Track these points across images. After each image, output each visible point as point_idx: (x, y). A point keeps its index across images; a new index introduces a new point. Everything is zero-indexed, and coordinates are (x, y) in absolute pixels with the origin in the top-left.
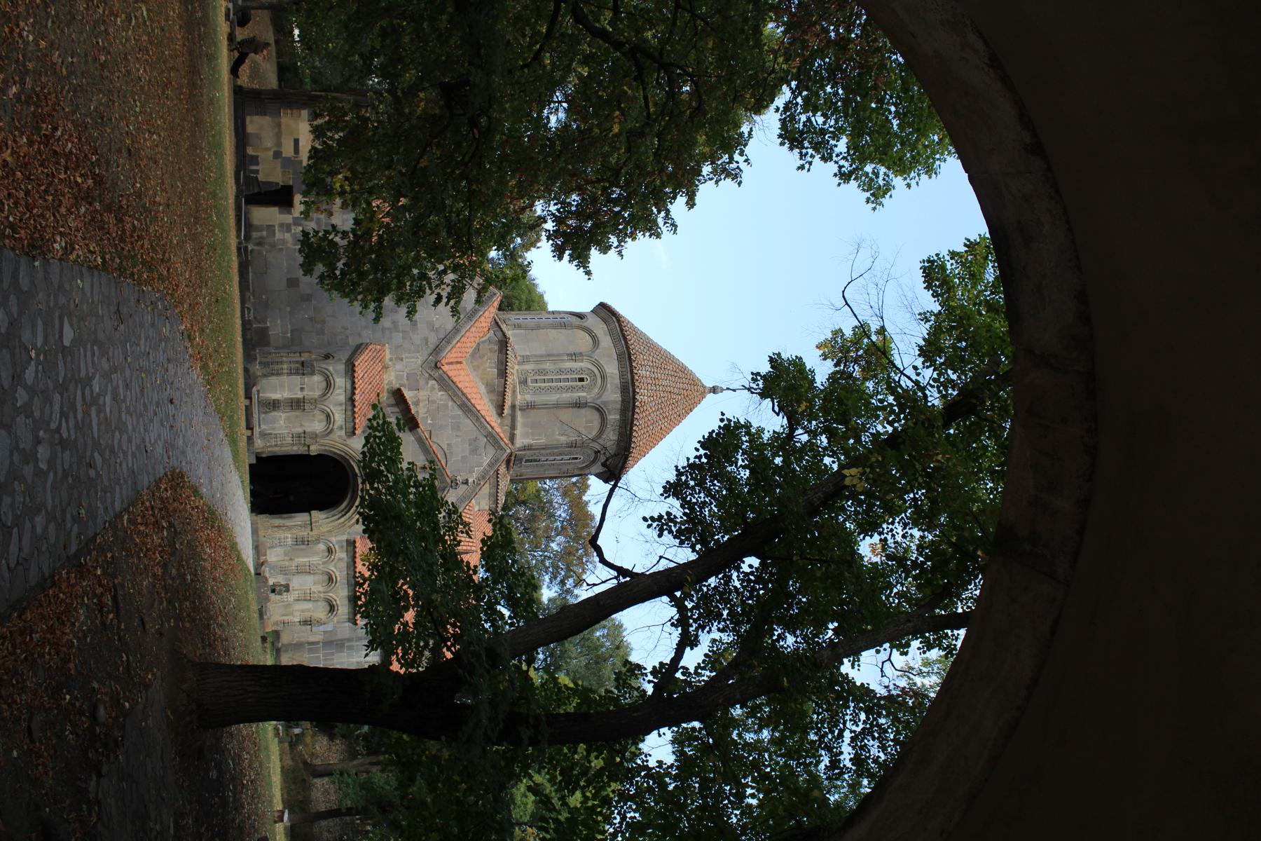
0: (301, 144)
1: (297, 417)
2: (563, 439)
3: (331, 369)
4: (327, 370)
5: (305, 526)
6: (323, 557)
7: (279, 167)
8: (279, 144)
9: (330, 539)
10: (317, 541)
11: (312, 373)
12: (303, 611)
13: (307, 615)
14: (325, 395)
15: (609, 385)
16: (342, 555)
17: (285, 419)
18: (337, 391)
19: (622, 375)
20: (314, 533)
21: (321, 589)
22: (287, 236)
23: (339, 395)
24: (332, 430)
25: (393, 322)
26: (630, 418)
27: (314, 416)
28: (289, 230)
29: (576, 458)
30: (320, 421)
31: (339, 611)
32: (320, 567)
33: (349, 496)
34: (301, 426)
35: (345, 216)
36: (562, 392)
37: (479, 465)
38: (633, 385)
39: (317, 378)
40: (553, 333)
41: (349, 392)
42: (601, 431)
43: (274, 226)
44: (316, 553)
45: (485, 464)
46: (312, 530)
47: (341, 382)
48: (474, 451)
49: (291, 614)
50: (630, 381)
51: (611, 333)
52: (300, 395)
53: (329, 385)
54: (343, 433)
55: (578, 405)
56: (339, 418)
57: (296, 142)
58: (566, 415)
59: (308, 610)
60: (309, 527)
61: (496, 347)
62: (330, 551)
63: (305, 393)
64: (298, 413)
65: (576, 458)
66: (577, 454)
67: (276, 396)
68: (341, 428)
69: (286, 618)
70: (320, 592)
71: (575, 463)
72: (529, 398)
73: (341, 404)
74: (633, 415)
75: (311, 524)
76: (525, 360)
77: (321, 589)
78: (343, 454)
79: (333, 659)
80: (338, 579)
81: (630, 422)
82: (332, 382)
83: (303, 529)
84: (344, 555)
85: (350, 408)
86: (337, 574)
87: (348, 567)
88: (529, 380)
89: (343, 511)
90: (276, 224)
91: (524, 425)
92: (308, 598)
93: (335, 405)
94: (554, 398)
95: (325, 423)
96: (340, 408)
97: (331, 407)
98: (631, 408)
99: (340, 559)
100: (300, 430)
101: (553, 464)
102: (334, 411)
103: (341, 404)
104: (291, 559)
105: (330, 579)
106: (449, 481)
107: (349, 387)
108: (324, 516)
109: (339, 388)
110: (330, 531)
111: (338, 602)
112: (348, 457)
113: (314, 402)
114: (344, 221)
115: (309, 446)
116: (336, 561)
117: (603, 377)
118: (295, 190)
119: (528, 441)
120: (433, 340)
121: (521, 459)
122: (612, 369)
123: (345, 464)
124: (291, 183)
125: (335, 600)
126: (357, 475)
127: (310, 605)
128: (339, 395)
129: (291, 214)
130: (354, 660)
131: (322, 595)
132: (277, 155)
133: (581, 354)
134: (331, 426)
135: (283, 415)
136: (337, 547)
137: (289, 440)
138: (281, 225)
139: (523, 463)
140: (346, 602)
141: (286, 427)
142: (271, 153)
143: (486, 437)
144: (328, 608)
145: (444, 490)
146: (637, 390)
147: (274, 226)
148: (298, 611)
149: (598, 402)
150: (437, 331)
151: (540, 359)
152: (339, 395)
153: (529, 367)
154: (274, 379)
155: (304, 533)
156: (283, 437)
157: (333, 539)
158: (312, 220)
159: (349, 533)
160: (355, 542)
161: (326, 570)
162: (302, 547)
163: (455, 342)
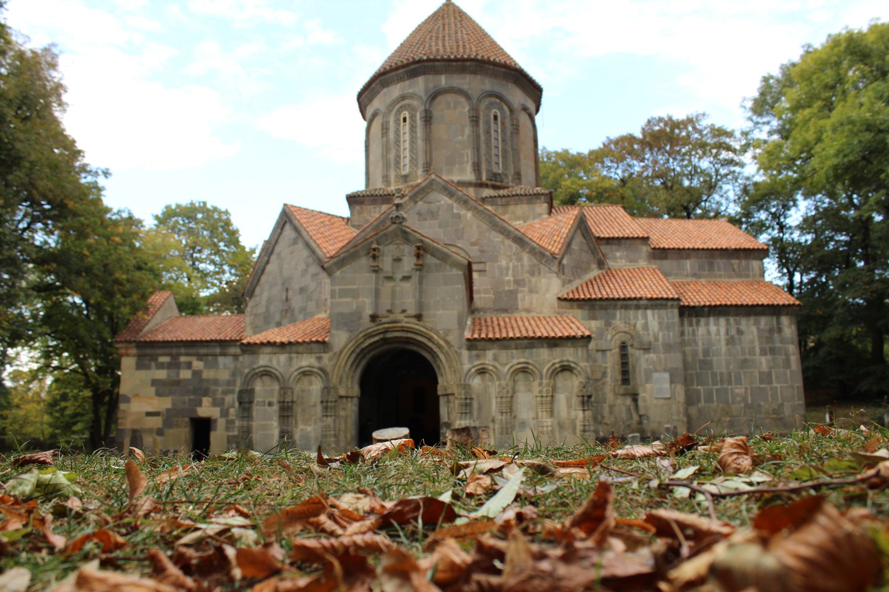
0: (150, 410)
1: (303, 411)
2: (468, 131)
3: (247, 371)
4: (247, 375)
5: (448, 402)
6: (492, 380)
7: (171, 431)
8: (150, 431)
9: (465, 372)
10: (466, 387)
11: (251, 392)
12: (569, 406)
13: (576, 401)
14: (277, 378)
15: (411, 91)
16: (489, 357)
17: (306, 424)
18: (274, 363)
19: (400, 79)
20: (455, 390)
21: (536, 383)
22: (237, 423)
23: (278, 363)
24: (321, 369)
25: (300, 312)
26: (442, 63)
27: (303, 391)
28: (232, 422)
29: (496, 117)
30: (311, 383)
31: (571, 359)
32: (503, 383)
33: (415, 348)
34: (315, 406)
35: (221, 366)
36: (416, 138)
37: (450, 207)
38: (407, 65)
39: (259, 387)
40: (372, 158)
41: (275, 350)
42: (460, 92)
43: (228, 437)
44: (486, 389)
45: (450, 201)
46: (453, 394)
47: (264, 360)
48: (433, 215)
49: (573, 422)
50: (406, 69)
51: (371, 100)
52: (276, 407)
53: (267, 373)
54: (326, 357)
55: (428, 119)
56: (307, 361)
57: (149, 414)
58: (440, 130)
59: (568, 400)
60: (451, 397)
61: (357, 208)
62: (482, 372)
63: (275, 400)
64: (298, 410)
65: (496, 117)
66: (488, 116)
67: (276, 433)
68: (319, 359)
69: (579, 428)
70: (540, 384)
71: (503, 118)
72: (420, 171)
73: (291, 359)
74: (438, 60)
75: (448, 395)
76: (386, 179)
77: (536, 383)
78: (354, 355)
79: (721, 373)
80: (522, 360)
81: (446, 63)
82: (262, 369)
83: (451, 405)
84: (490, 354)
85: (294, 348)
86: (515, 361)
87: (506, 348)
88: (403, 173)
89: (433, 356)
90: (226, 434)
91: (450, 172)
92: (549, 402)
93: (290, 365)
94: (420, 143)
95: (313, 378)
96: (295, 360)
97: (292, 370)
98: (431, 64)
99: (495, 358)
100: (319, 408)
101: (504, 141)
102: (296, 367)
103: (291, 359)
104: (493, 421)
105: (524, 370)
106: (394, 226)
107: (268, 350)
108: (440, 380)
109: (271, 360)
110: (455, 371)
111: (557, 360)
112: (358, 350)
113: (285, 389)
114: (225, 367)
115: (341, 397)
116: (497, 364)
117: (403, 98)
118: (193, 416)
119: (469, 168)
120: (315, 269)
121: (495, 175)
122: (395, 91)
123: (373, 353)
124: (187, 420)
125: (554, 364)
126: (382, 339)
127: (561, 399)
128: (278, 363)
129: (216, 420)
130: (724, 348)
131: (545, 381)
132: (160, 432)
133: (382, 125)
134: (315, 370)
135: (301, 426)
136: (476, 363)
137: (329, 421)
138: (227, 429)
139: (500, 172)
140: (558, 351)
141: (315, 423)
142: (159, 438)
143: (416, 202)
144: (567, 374)
145: (405, 232)
146: (411, 60)
147: (228, 437)
148: (569, 413)
149: (425, 98)
150: (307, 266)
151: (387, 166)
152: (279, 362)
153: (392, 175)
154: (256, 436)
155: (456, 404)
156: (327, 427)
157: (467, 366)
158: (223, 399)
159: (460, 348)
160: (468, 340)
161: (508, 377)
162: (475, 404)
163: (314, 245)
